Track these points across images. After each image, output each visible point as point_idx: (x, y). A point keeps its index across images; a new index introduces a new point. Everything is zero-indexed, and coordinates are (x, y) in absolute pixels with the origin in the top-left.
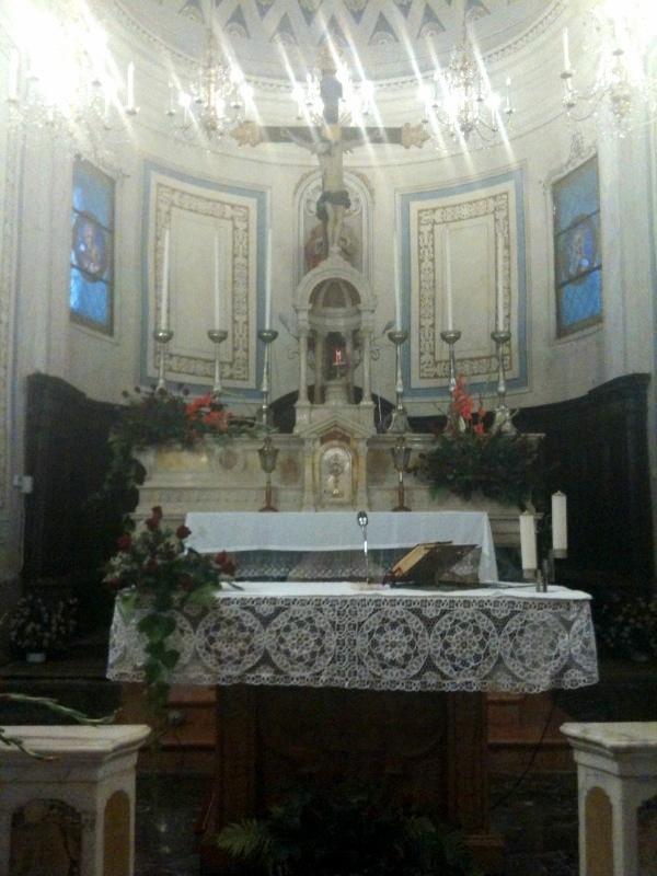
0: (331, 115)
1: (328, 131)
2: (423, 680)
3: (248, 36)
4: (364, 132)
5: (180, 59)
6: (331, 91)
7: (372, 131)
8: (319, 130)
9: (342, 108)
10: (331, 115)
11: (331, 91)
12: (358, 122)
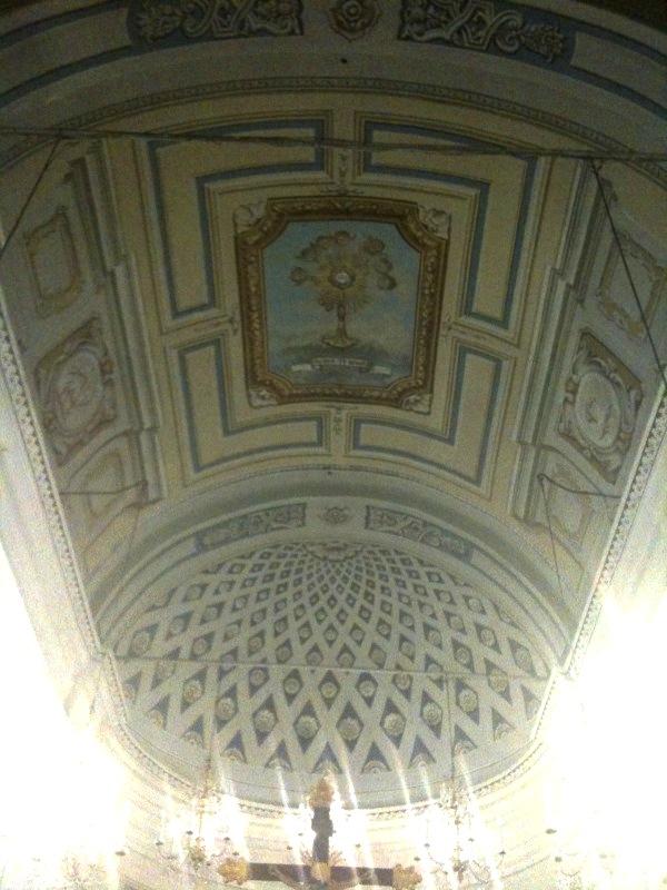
0: (321, 849)
1: (320, 872)
2: (383, 257)
3: (245, 761)
4: (355, 873)
5: (177, 783)
6: (322, 823)
7: (363, 872)
8: (307, 869)
9: (334, 843)
10: (321, 849)
11: (322, 823)
12: (350, 861)
